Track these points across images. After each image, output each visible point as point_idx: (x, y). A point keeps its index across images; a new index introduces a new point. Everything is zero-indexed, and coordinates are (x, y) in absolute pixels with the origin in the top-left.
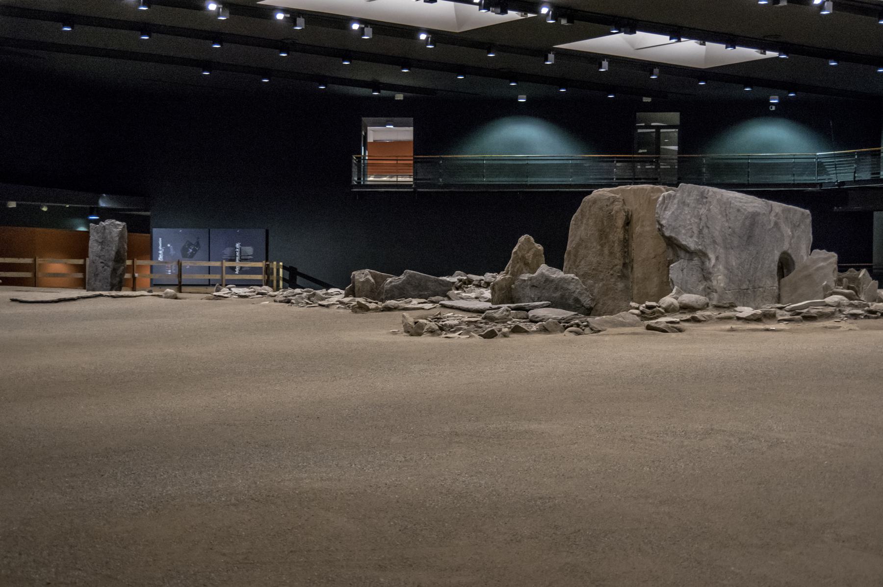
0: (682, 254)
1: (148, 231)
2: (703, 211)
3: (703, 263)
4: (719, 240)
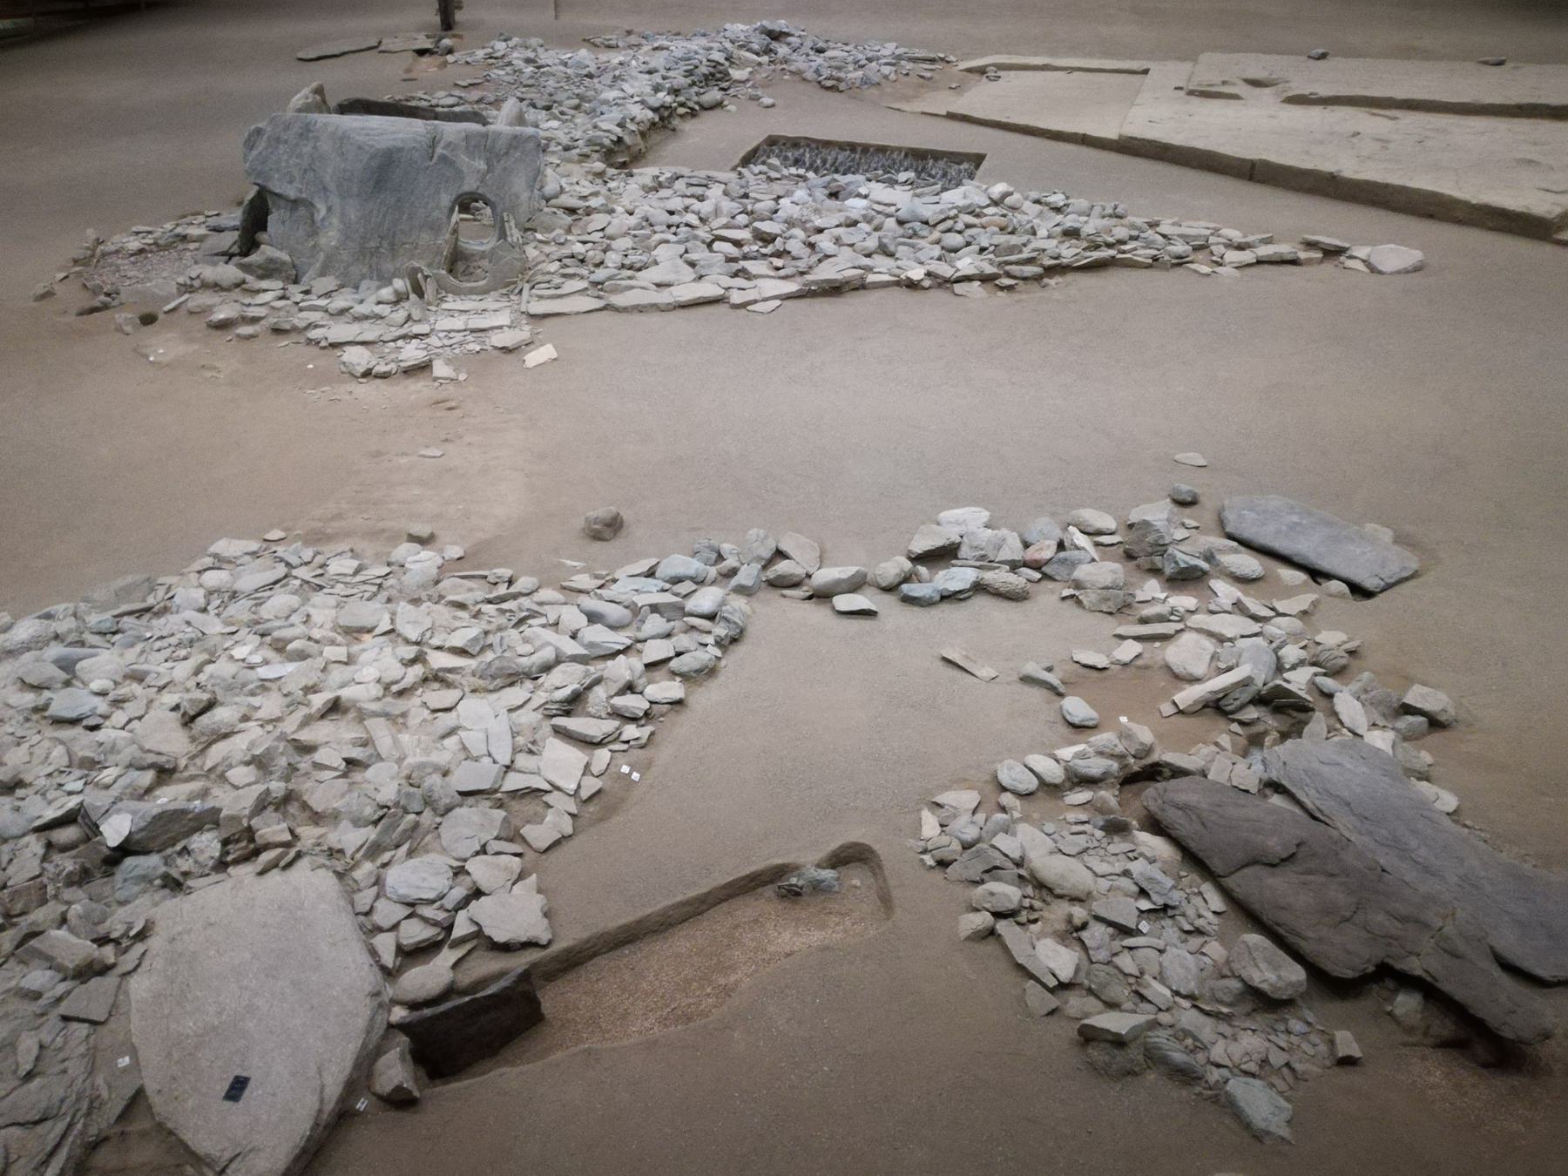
0: (282, 203)
2: (307, 149)
4: (332, 186)
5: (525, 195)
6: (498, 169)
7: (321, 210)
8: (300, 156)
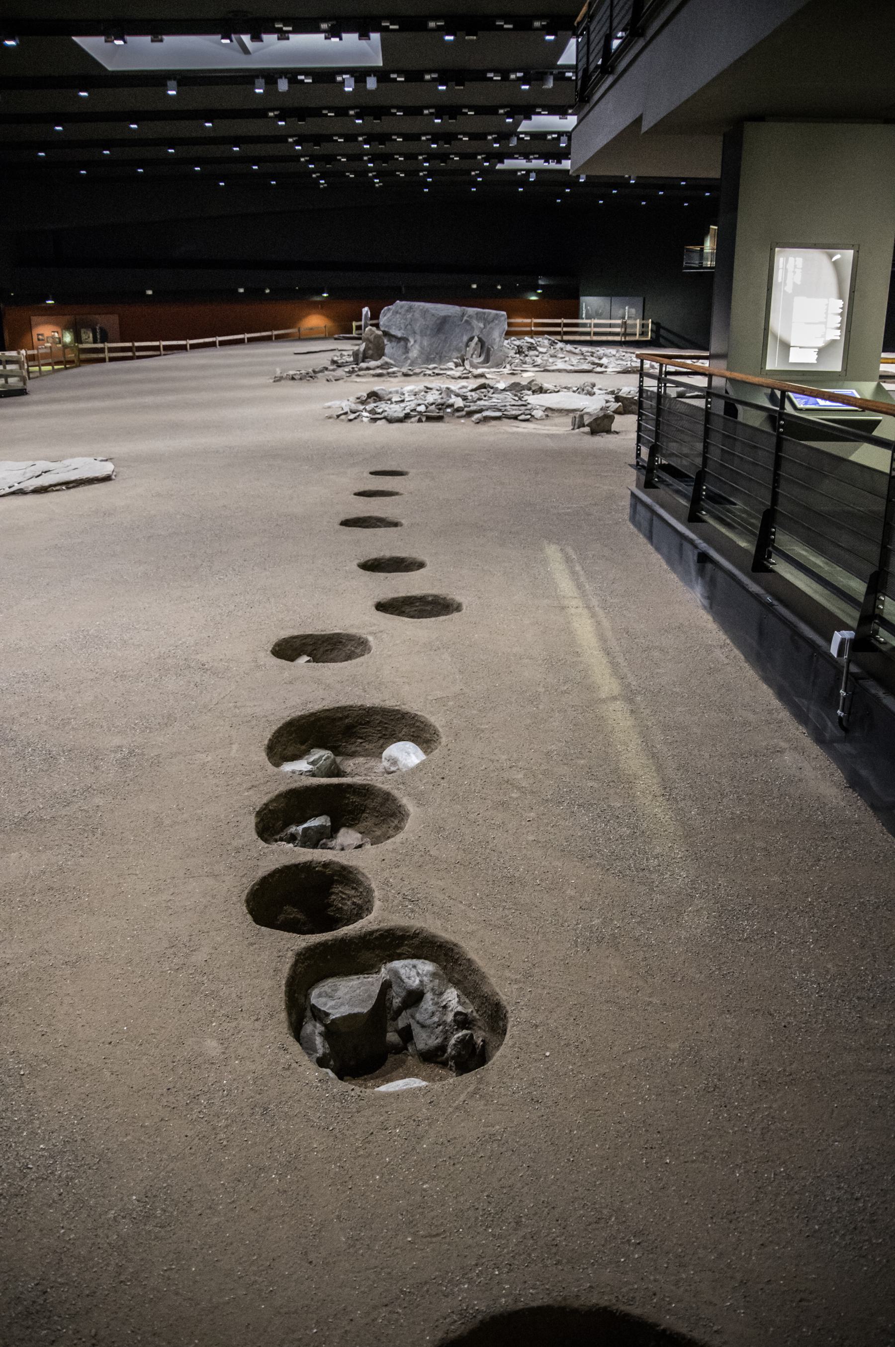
0: (394, 339)
1: (578, 299)
2: (409, 316)
4: (418, 331)
5: (497, 340)
6: (488, 327)
8: (406, 319)
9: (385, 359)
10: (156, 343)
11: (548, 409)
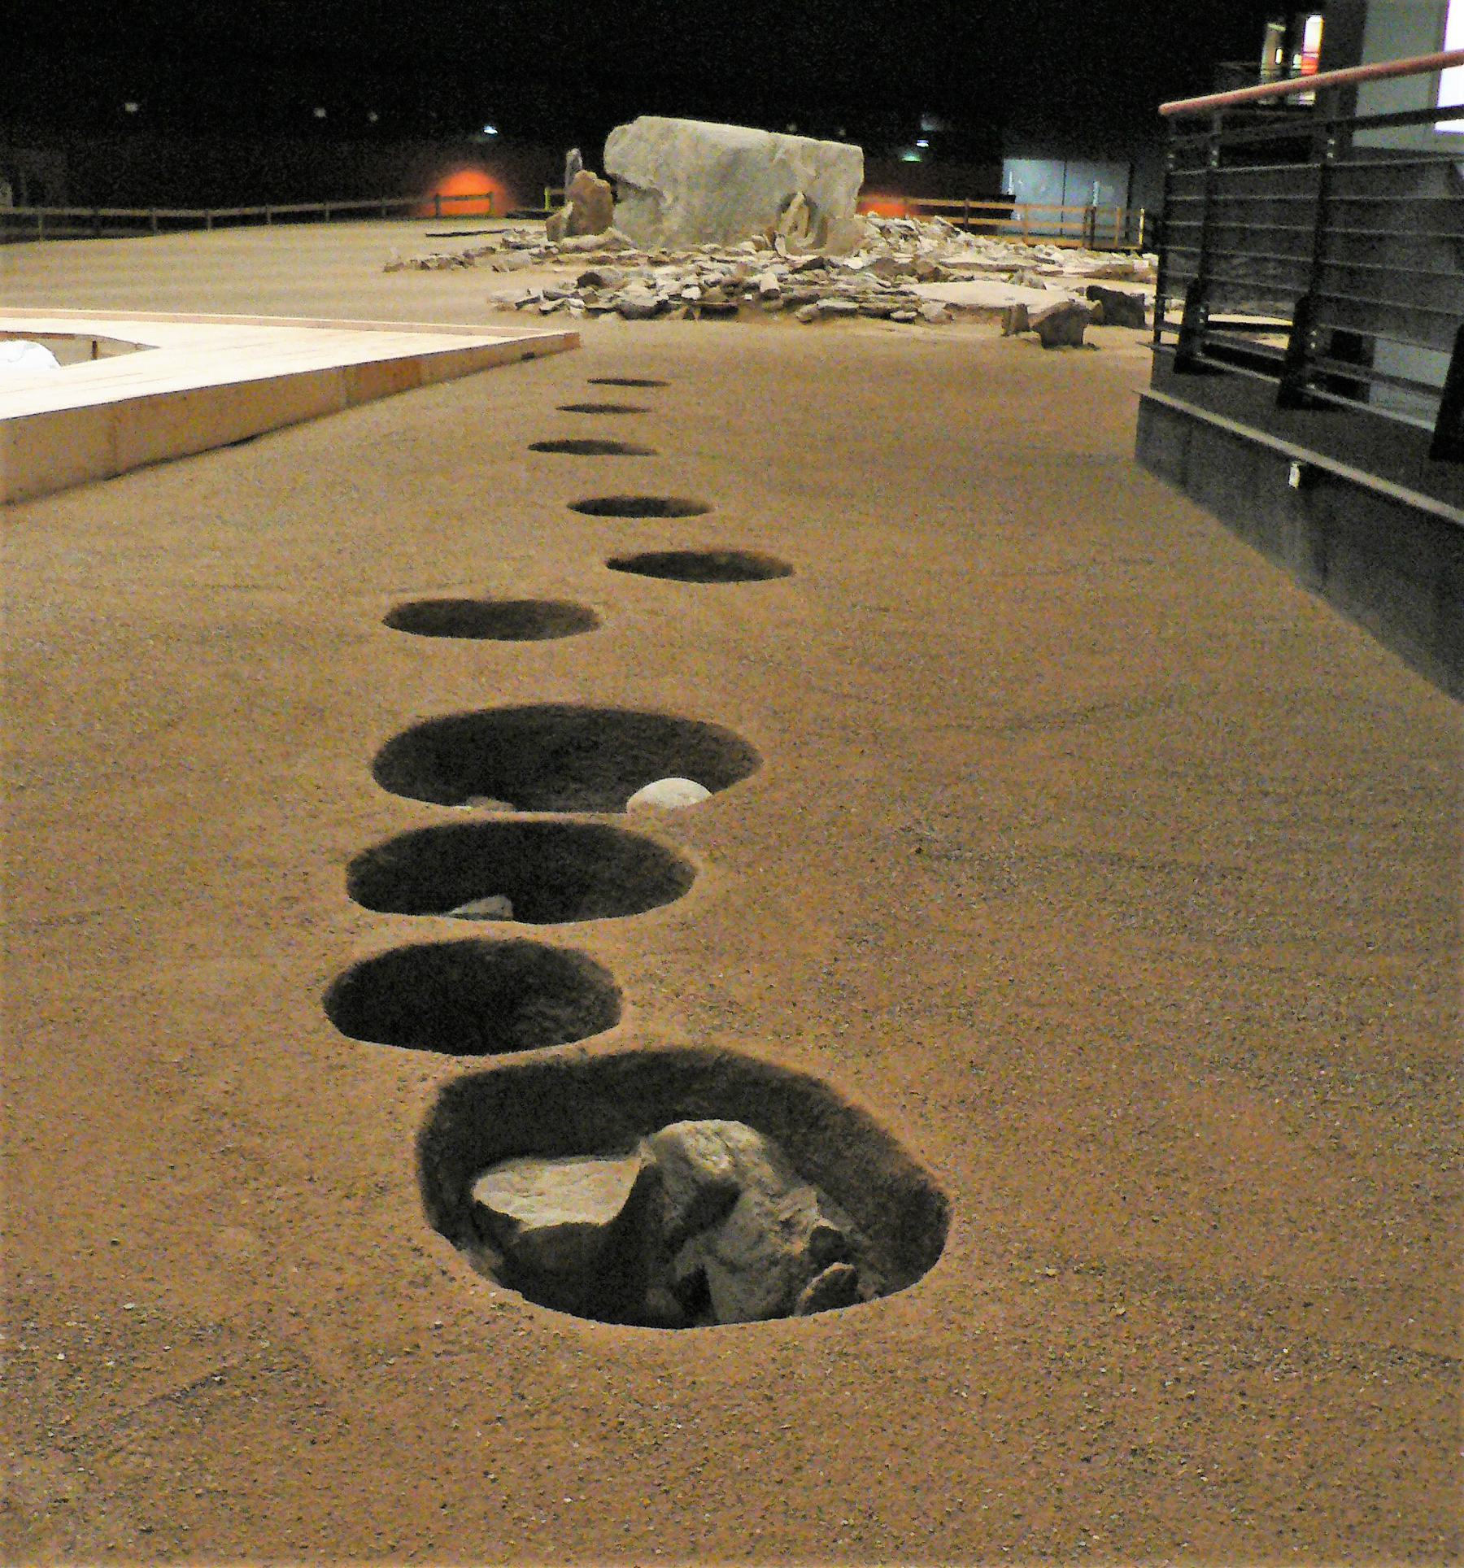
0: (632, 192)
1: (1001, 164)
2: (665, 146)
3: (658, 204)
7: (669, 198)
9: (613, 231)
10: (144, 213)
11: (951, 306)
